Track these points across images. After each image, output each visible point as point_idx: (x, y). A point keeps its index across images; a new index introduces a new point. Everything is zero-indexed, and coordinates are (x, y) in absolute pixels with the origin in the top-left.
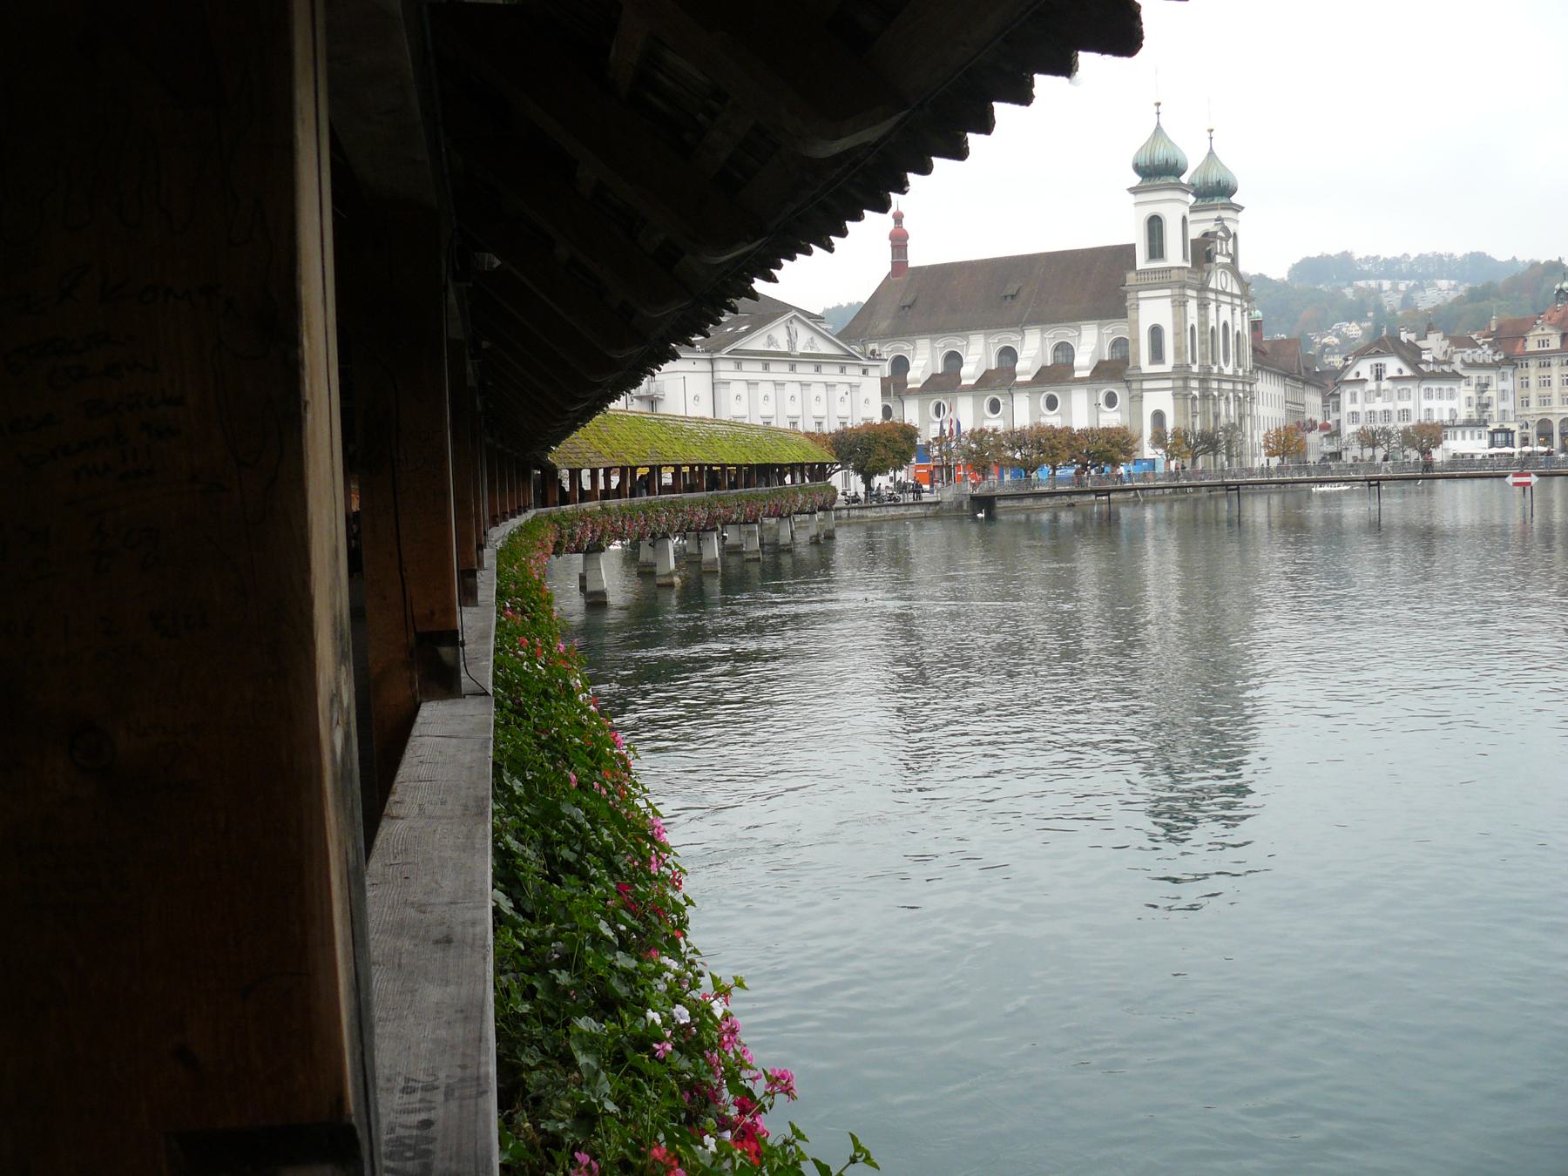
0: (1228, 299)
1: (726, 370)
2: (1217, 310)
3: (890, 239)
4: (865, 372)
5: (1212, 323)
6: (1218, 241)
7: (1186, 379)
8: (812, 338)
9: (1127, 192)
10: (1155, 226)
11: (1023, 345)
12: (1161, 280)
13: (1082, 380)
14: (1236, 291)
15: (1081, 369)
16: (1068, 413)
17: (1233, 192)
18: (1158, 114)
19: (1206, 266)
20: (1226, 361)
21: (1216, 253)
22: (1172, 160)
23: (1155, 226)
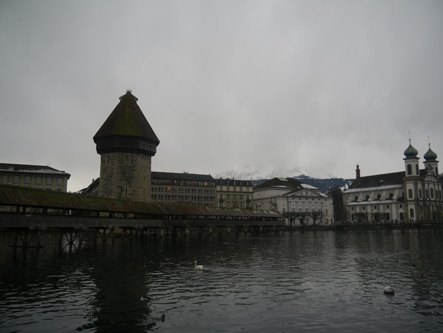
0: (433, 183)
1: (290, 200)
2: (428, 185)
3: (356, 171)
6: (429, 170)
7: (418, 201)
8: (312, 193)
9: (403, 160)
10: (409, 167)
11: (382, 193)
12: (411, 179)
14: (435, 180)
16: (391, 210)
17: (436, 157)
18: (410, 142)
20: (432, 197)
21: (428, 172)
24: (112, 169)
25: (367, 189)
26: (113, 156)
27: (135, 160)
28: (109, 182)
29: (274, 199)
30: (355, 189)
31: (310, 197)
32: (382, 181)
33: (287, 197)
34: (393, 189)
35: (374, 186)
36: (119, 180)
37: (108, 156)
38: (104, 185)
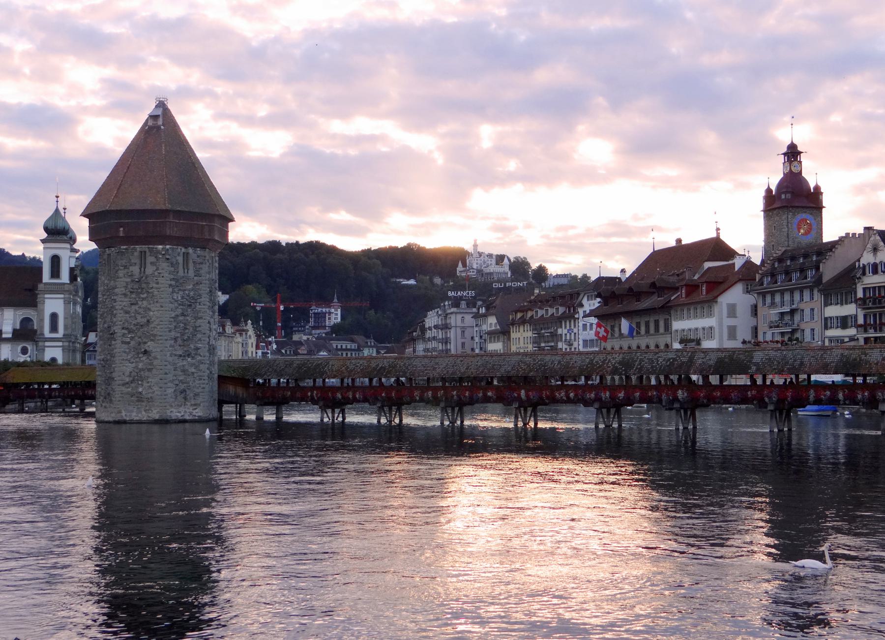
10: (55, 261)
13: (7, 340)
15: (6, 333)
18: (57, 201)
24: (197, 283)
26: (198, 256)
28: (189, 310)
37: (184, 253)
38: (177, 316)
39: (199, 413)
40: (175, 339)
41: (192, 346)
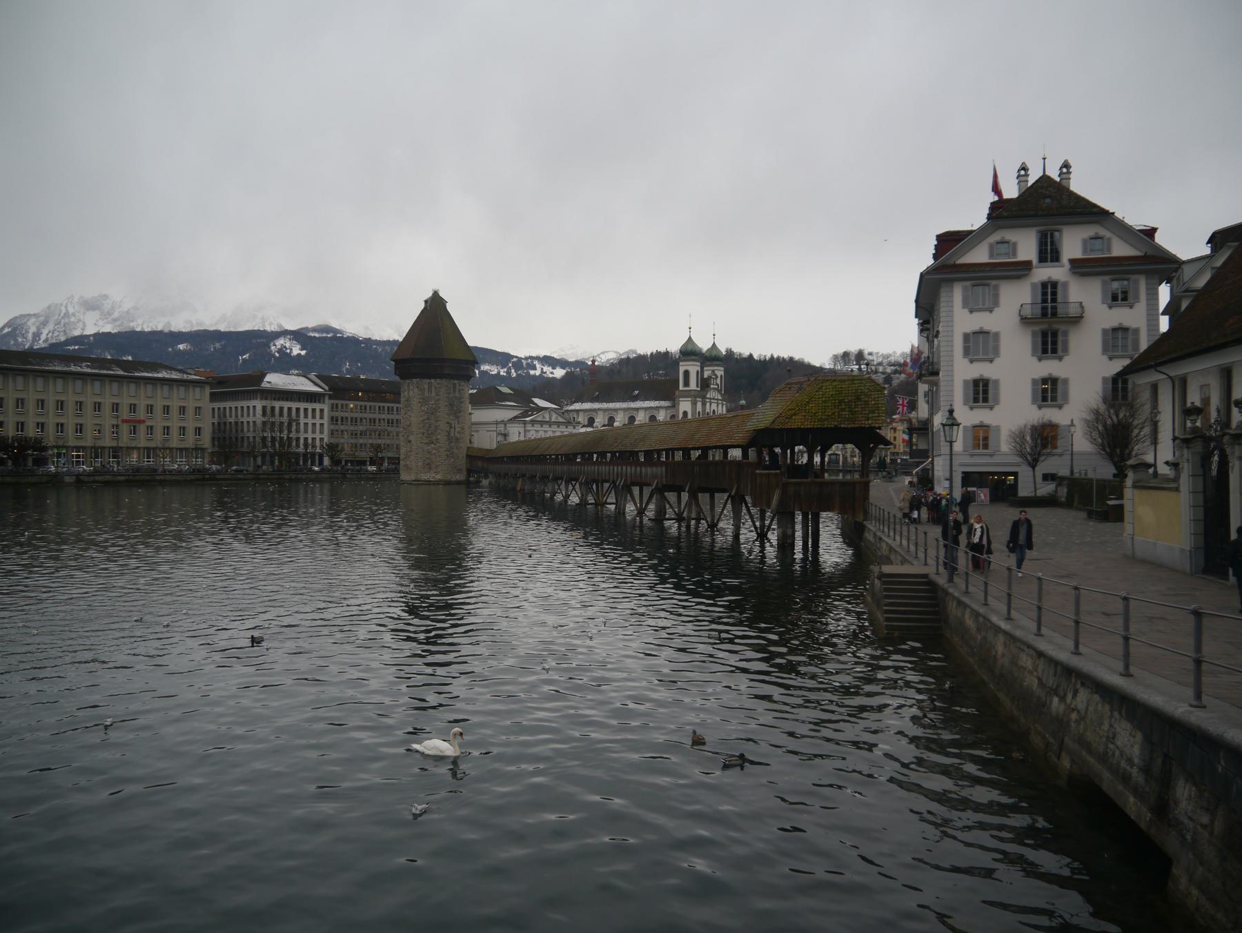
0: (716, 401)
1: (529, 427)
2: (710, 406)
4: (574, 428)
5: (708, 410)
12: (687, 394)
14: (720, 397)
19: (706, 389)
22: (694, 351)
23: (687, 373)
25: (611, 405)
27: (463, 390)
29: (503, 425)
30: (589, 403)
31: (555, 423)
32: (637, 392)
33: (525, 423)
34: (657, 408)
35: (624, 401)
36: (448, 414)
39: (439, 477)
40: (423, 433)
41: (434, 438)
